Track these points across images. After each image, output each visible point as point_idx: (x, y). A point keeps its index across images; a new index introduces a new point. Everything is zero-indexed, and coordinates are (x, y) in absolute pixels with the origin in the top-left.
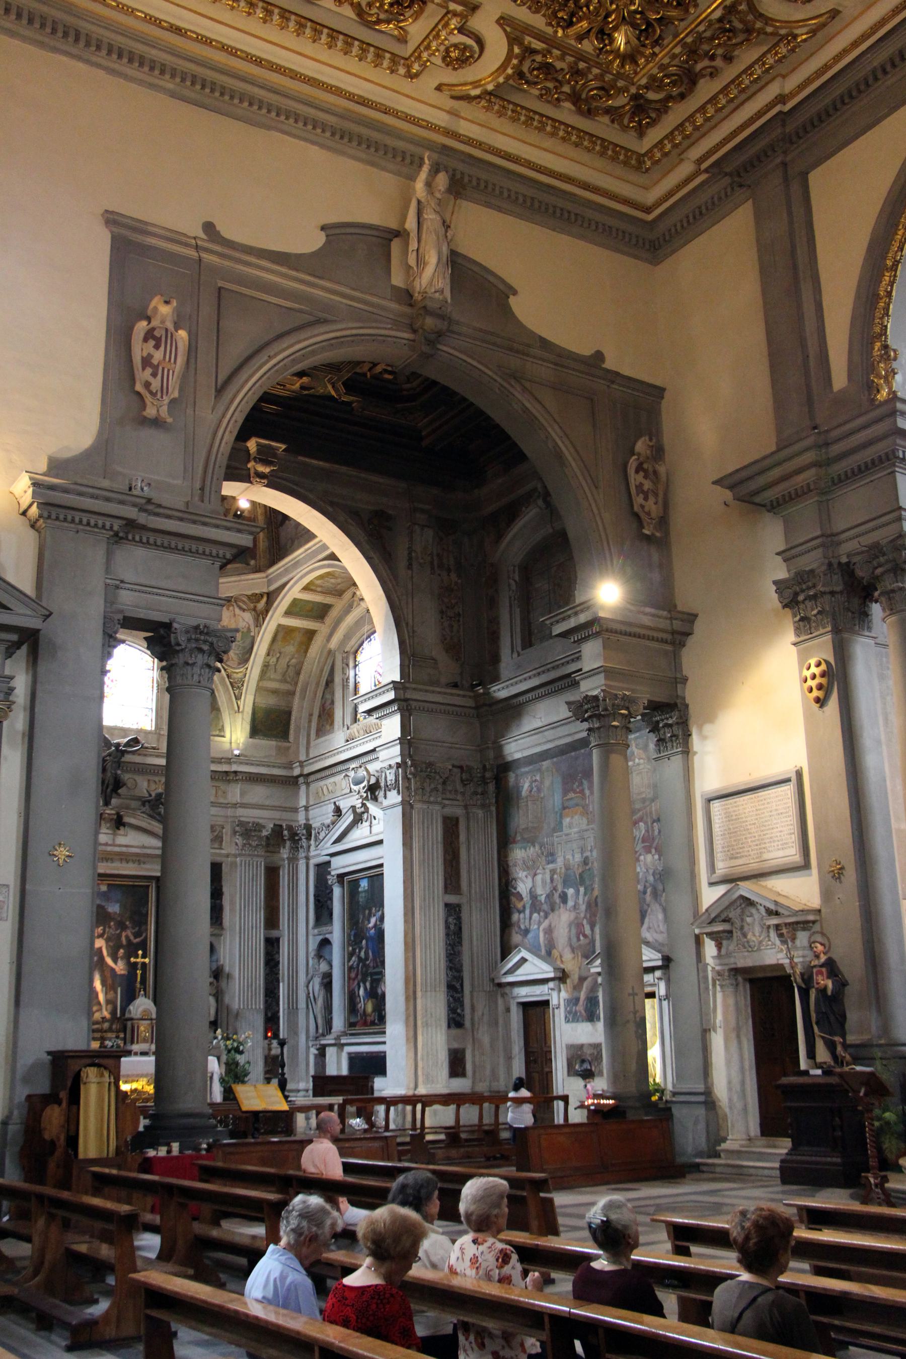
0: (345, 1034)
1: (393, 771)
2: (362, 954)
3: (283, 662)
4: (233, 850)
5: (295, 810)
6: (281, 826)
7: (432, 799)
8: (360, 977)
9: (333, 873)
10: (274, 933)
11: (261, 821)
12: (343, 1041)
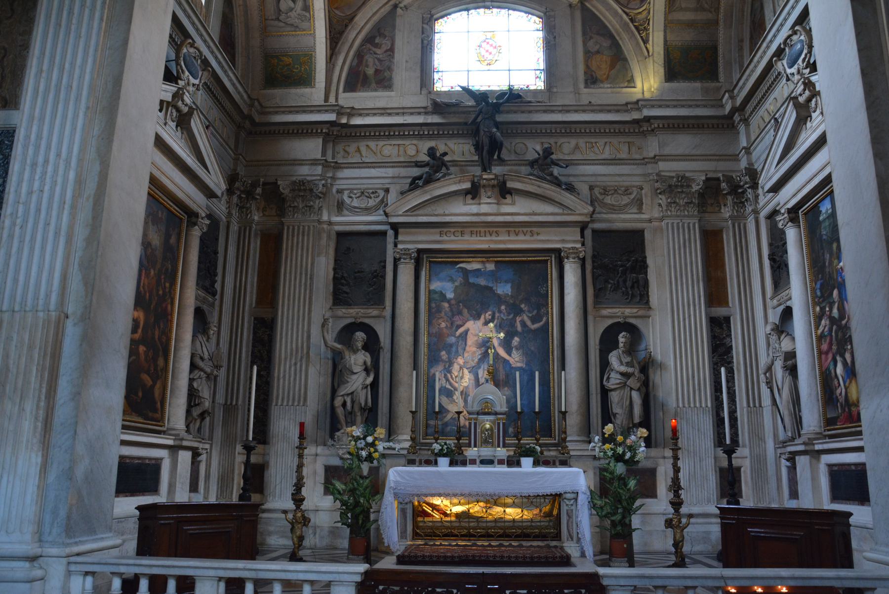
0: (821, 436)
4: (656, 214)
5: (735, 158)
6: (718, 179)
8: (834, 348)
9: (783, 211)
10: (721, 311)
11: (687, 175)
12: (817, 447)
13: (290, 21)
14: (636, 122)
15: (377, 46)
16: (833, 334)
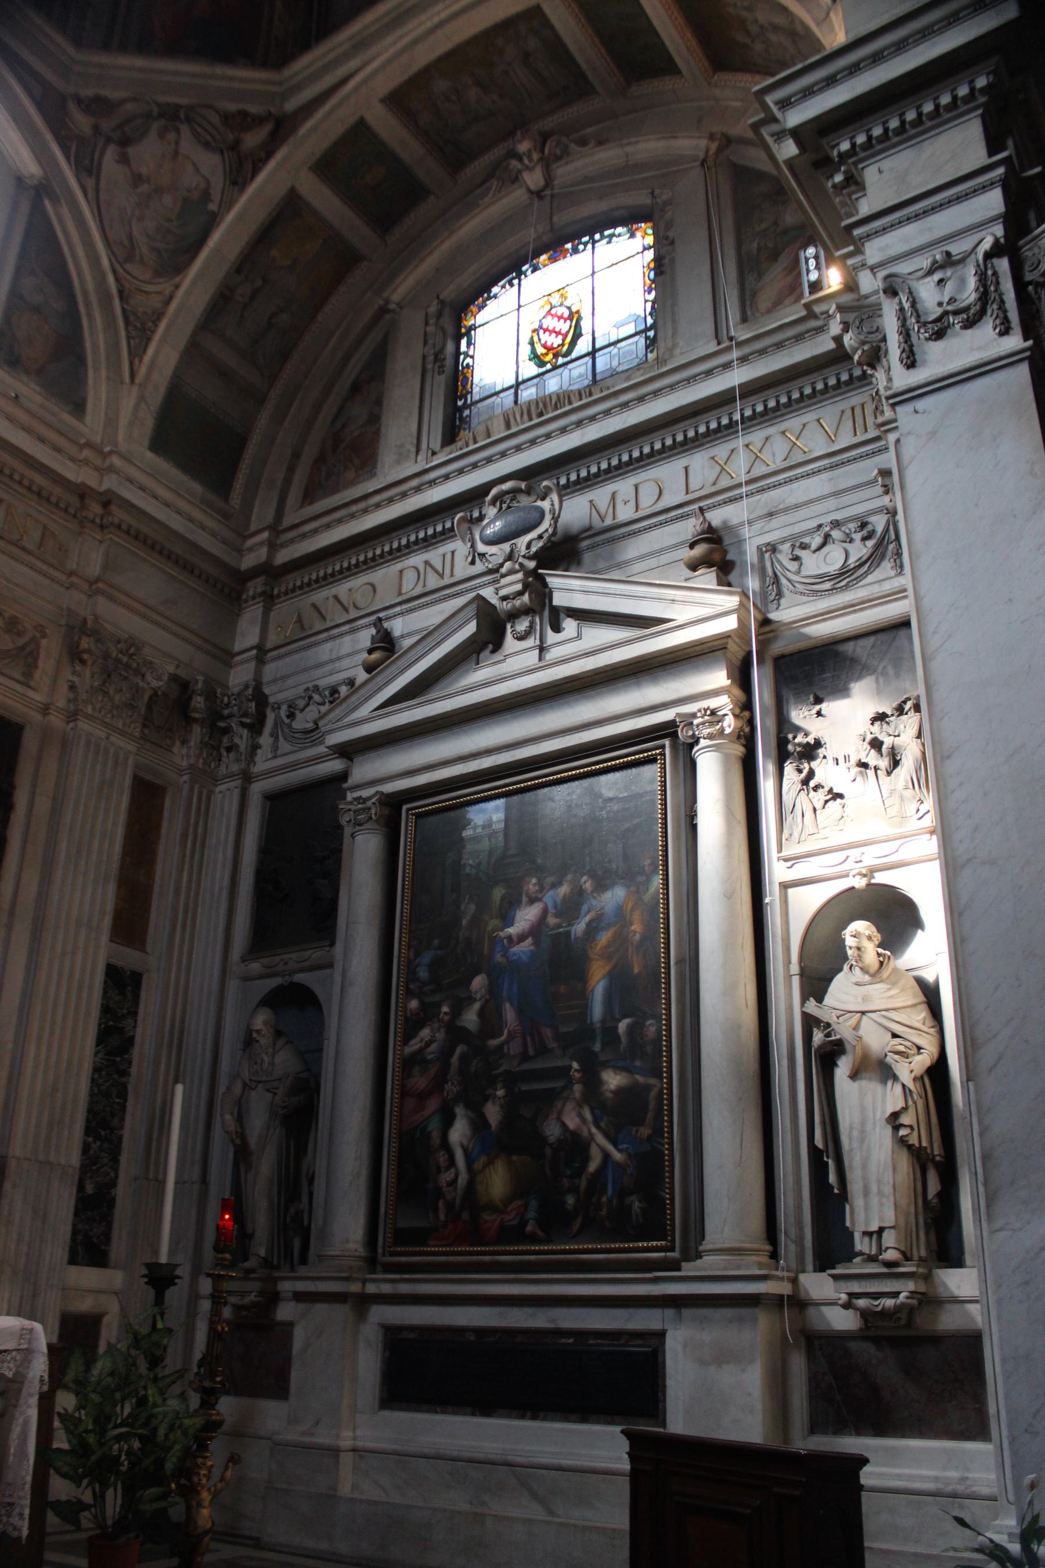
2: (470, 1018)
8: (452, 1088)
14: (83, 493)
16: (455, 1060)
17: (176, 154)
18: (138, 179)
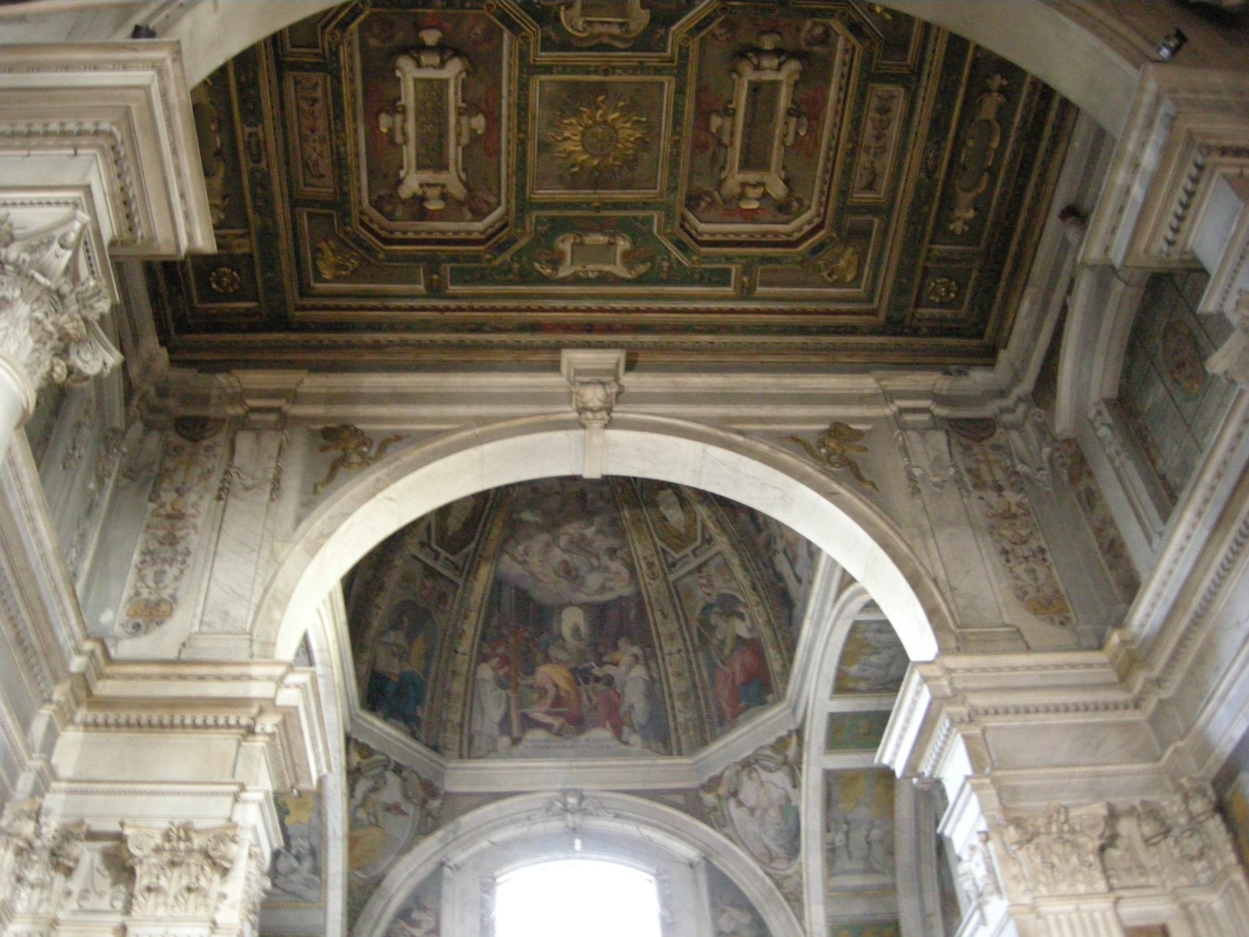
1: (978, 857)
3: (858, 837)
7: (1082, 888)
13: (289, 887)
15: (415, 924)
17: (762, 784)
18: (752, 811)
